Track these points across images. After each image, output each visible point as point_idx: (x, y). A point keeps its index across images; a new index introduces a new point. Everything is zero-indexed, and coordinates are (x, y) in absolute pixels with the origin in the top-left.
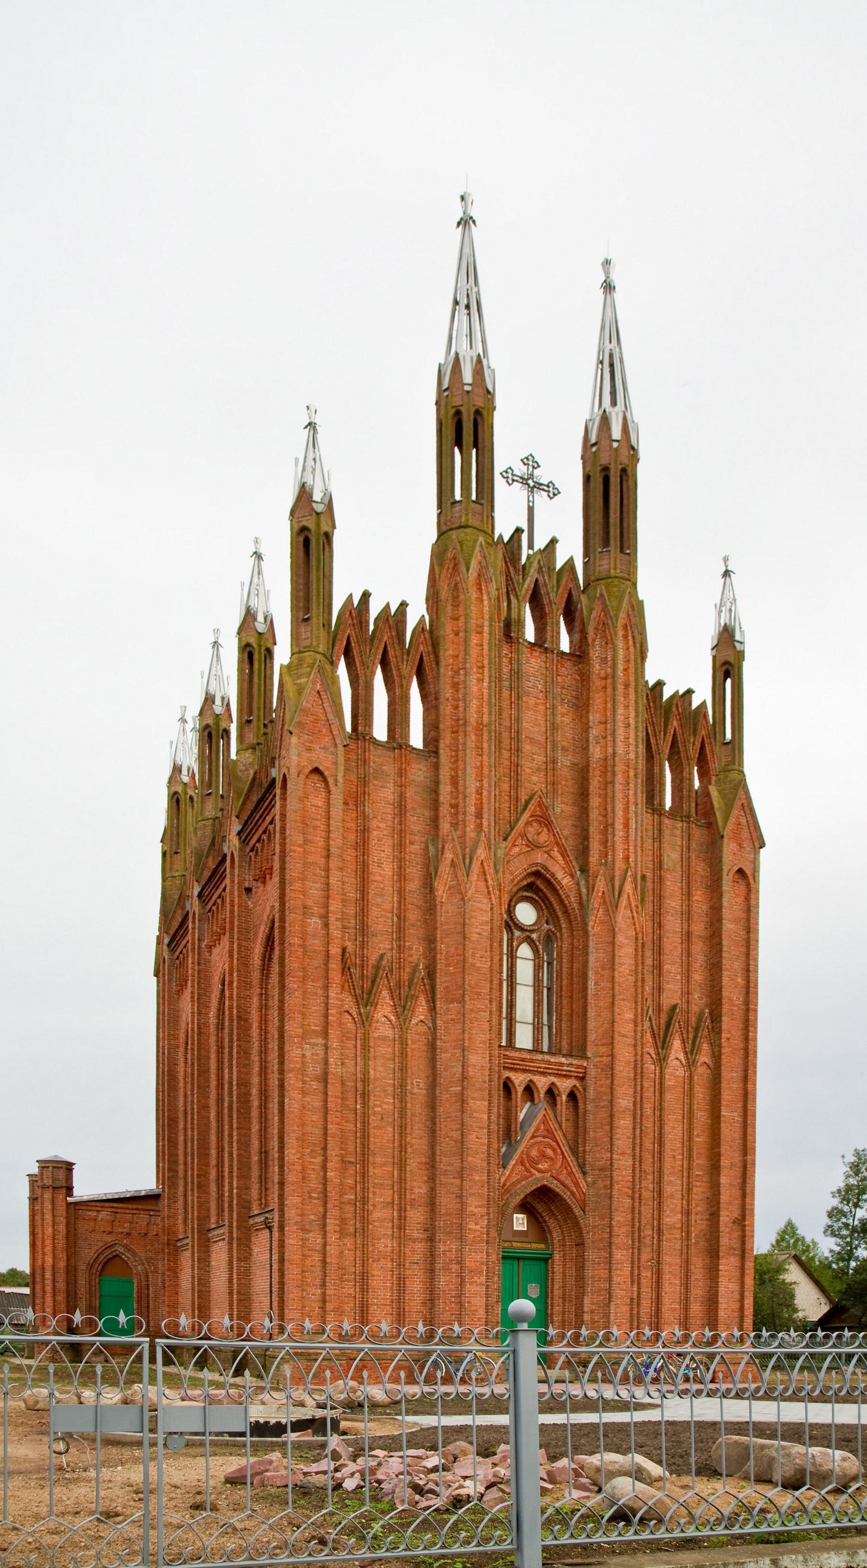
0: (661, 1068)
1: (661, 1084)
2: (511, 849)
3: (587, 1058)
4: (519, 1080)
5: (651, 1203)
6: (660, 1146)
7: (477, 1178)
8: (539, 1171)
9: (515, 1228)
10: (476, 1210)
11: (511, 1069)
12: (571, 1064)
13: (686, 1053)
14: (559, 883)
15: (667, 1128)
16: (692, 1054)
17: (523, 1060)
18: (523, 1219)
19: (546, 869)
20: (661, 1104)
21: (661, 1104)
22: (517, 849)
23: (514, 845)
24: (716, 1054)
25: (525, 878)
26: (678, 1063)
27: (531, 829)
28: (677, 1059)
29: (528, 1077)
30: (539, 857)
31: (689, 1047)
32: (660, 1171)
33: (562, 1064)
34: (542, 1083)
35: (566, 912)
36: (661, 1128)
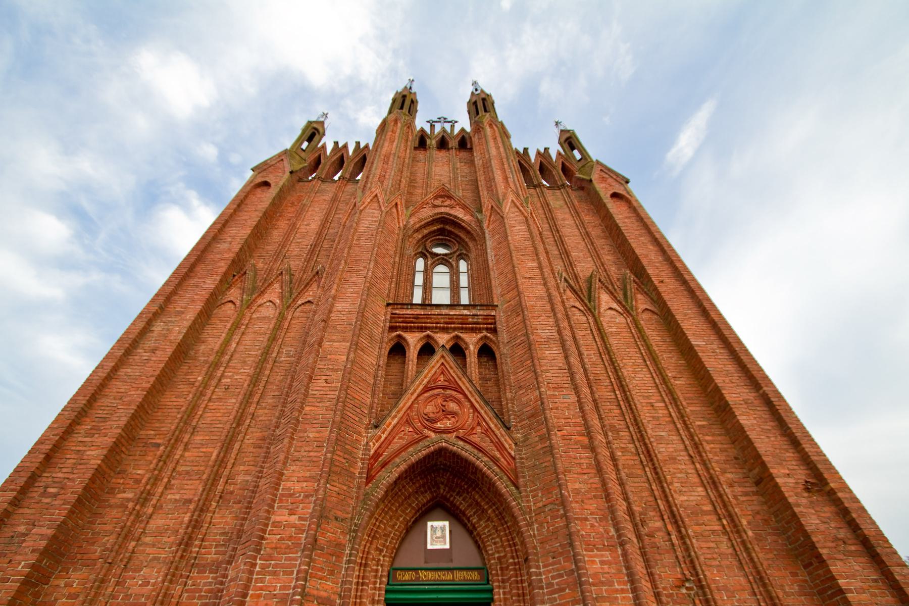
0: (594, 316)
1: (599, 330)
5: (639, 472)
6: (624, 392)
7: (311, 435)
8: (437, 431)
9: (429, 547)
10: (297, 487)
13: (619, 302)
15: (626, 372)
16: (627, 302)
18: (443, 529)
20: (607, 348)
21: (607, 348)
24: (655, 298)
26: (613, 312)
28: (610, 309)
31: (621, 297)
32: (637, 423)
35: (468, 232)
36: (616, 371)
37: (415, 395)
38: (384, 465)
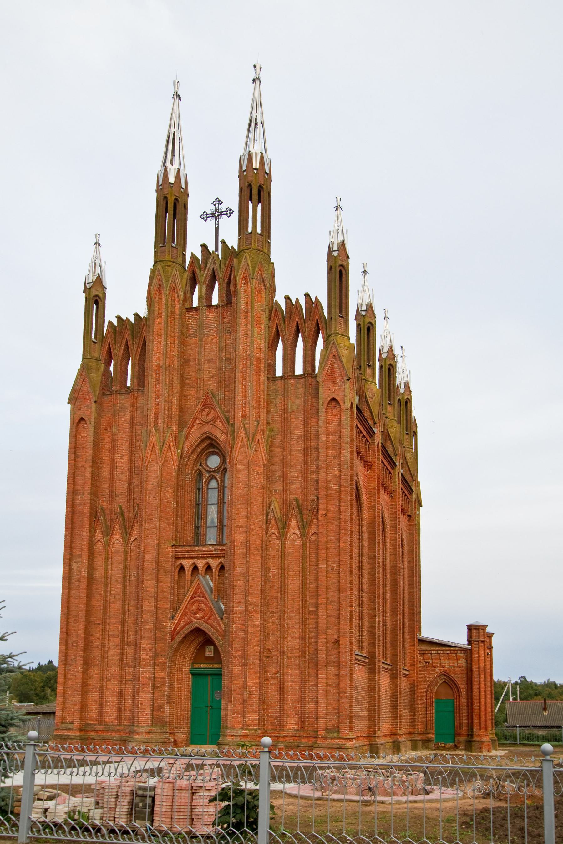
2: (191, 428)
3: (225, 544)
4: (187, 564)
8: (196, 618)
11: (184, 558)
12: (215, 550)
14: (220, 440)
17: (188, 552)
19: (212, 434)
22: (195, 427)
23: (193, 426)
25: (202, 441)
27: (204, 413)
29: (191, 561)
30: (207, 428)
33: (211, 551)
34: (201, 563)
37: (187, 601)
38: (178, 633)
